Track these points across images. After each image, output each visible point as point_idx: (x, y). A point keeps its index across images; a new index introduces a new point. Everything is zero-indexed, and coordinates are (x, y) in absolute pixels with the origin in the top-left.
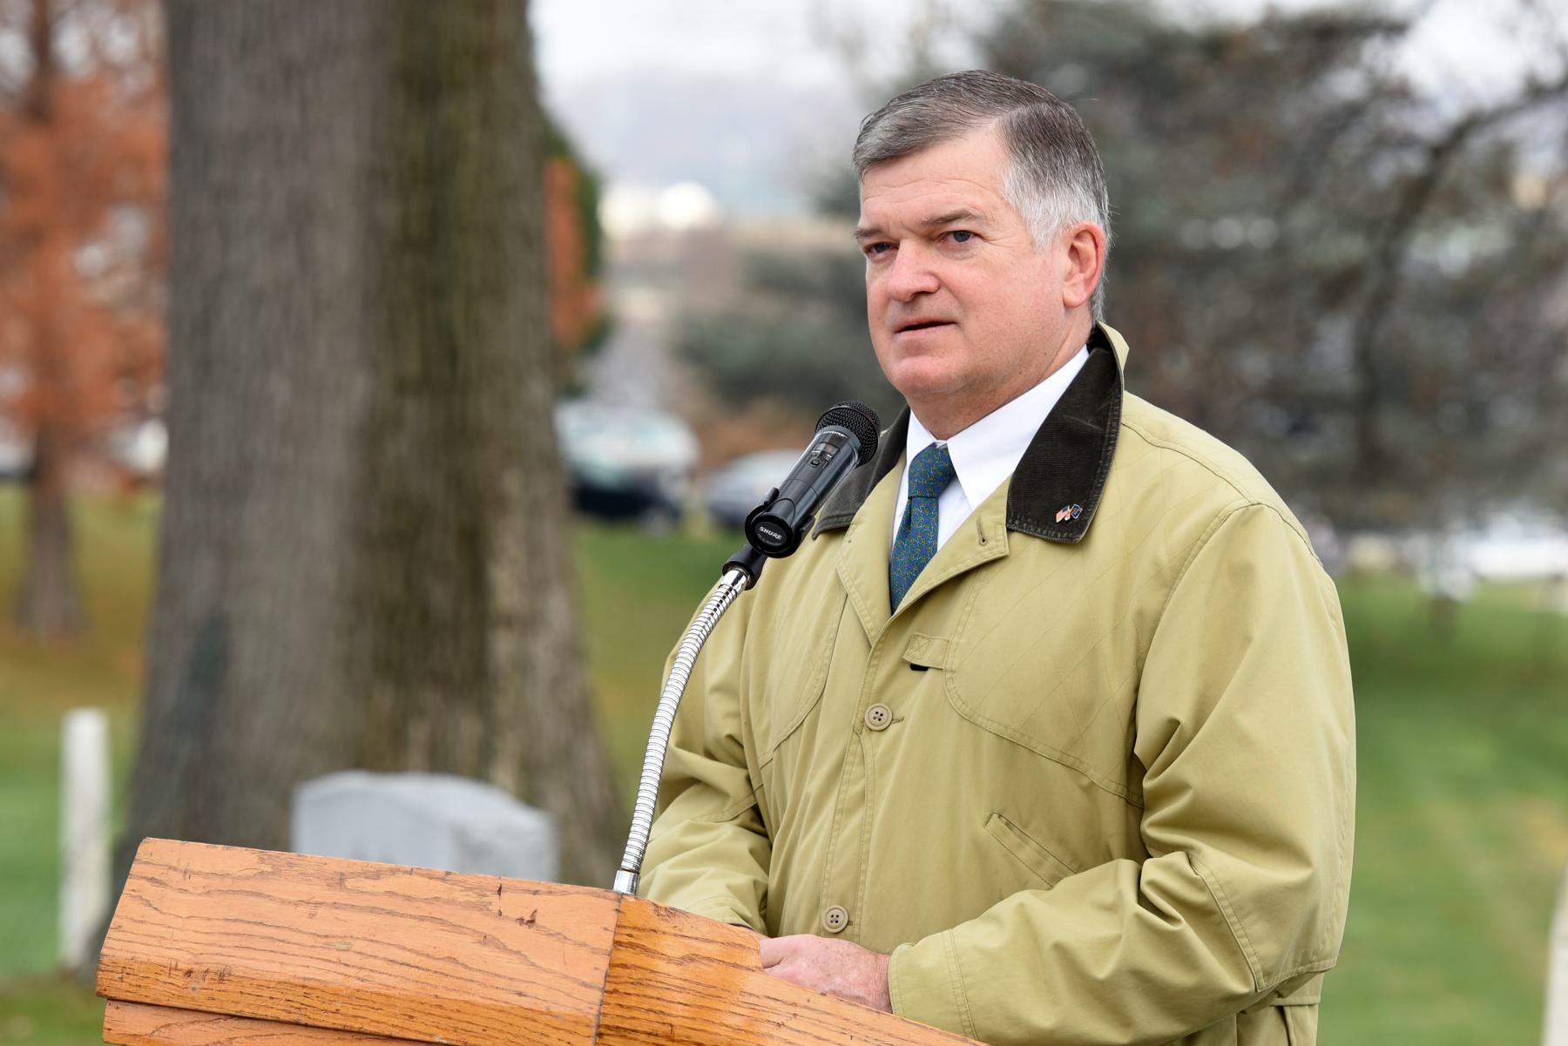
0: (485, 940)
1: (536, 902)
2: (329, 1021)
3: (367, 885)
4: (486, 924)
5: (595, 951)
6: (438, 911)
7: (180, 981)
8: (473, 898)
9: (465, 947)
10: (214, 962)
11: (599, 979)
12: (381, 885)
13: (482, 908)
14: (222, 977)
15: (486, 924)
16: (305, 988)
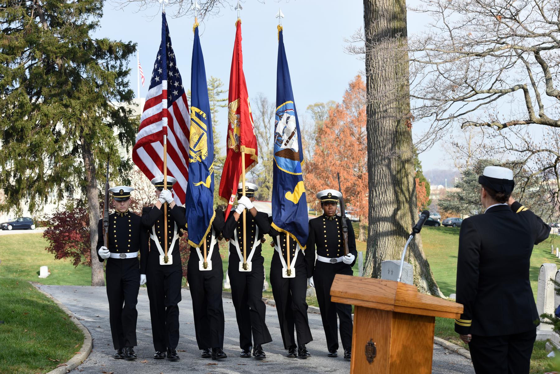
0: (380, 288)
1: (387, 283)
2: (360, 299)
3: (365, 280)
4: (380, 286)
5: (394, 289)
6: (374, 284)
7: (341, 293)
8: (378, 282)
9: (377, 289)
10: (345, 291)
11: (395, 293)
12: (367, 280)
13: (380, 283)
14: (346, 293)
15: (380, 286)
16: (357, 294)
